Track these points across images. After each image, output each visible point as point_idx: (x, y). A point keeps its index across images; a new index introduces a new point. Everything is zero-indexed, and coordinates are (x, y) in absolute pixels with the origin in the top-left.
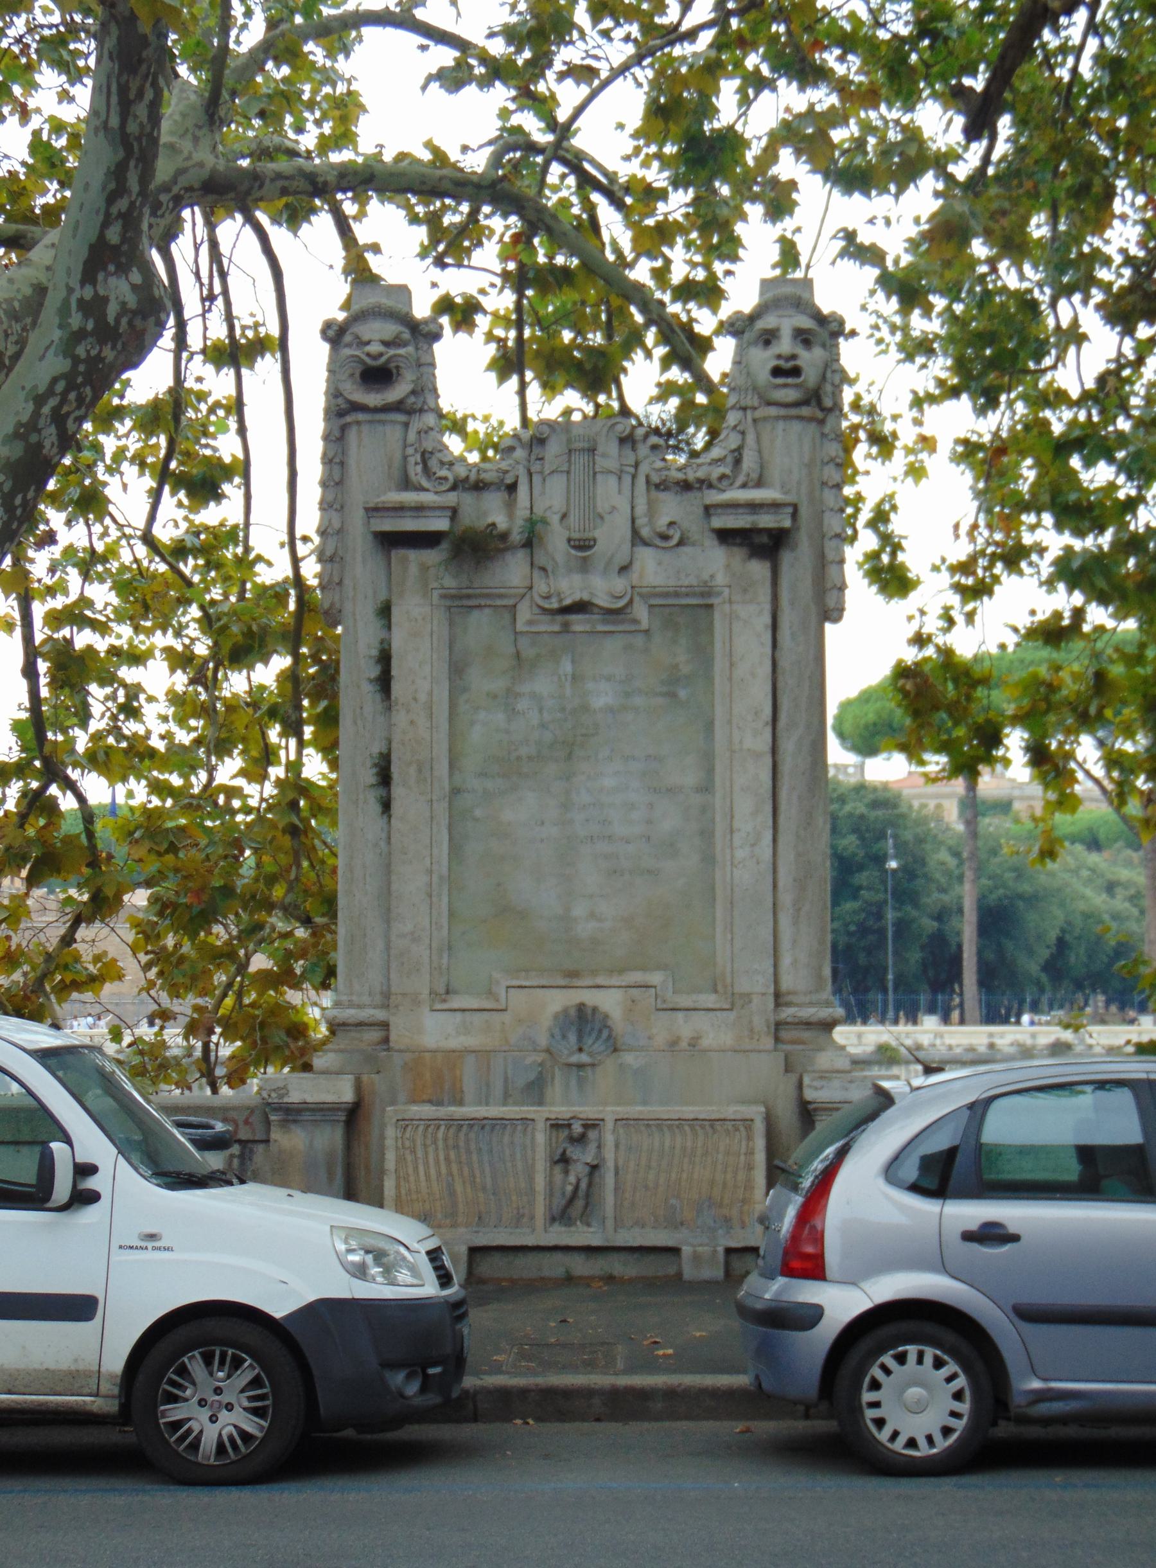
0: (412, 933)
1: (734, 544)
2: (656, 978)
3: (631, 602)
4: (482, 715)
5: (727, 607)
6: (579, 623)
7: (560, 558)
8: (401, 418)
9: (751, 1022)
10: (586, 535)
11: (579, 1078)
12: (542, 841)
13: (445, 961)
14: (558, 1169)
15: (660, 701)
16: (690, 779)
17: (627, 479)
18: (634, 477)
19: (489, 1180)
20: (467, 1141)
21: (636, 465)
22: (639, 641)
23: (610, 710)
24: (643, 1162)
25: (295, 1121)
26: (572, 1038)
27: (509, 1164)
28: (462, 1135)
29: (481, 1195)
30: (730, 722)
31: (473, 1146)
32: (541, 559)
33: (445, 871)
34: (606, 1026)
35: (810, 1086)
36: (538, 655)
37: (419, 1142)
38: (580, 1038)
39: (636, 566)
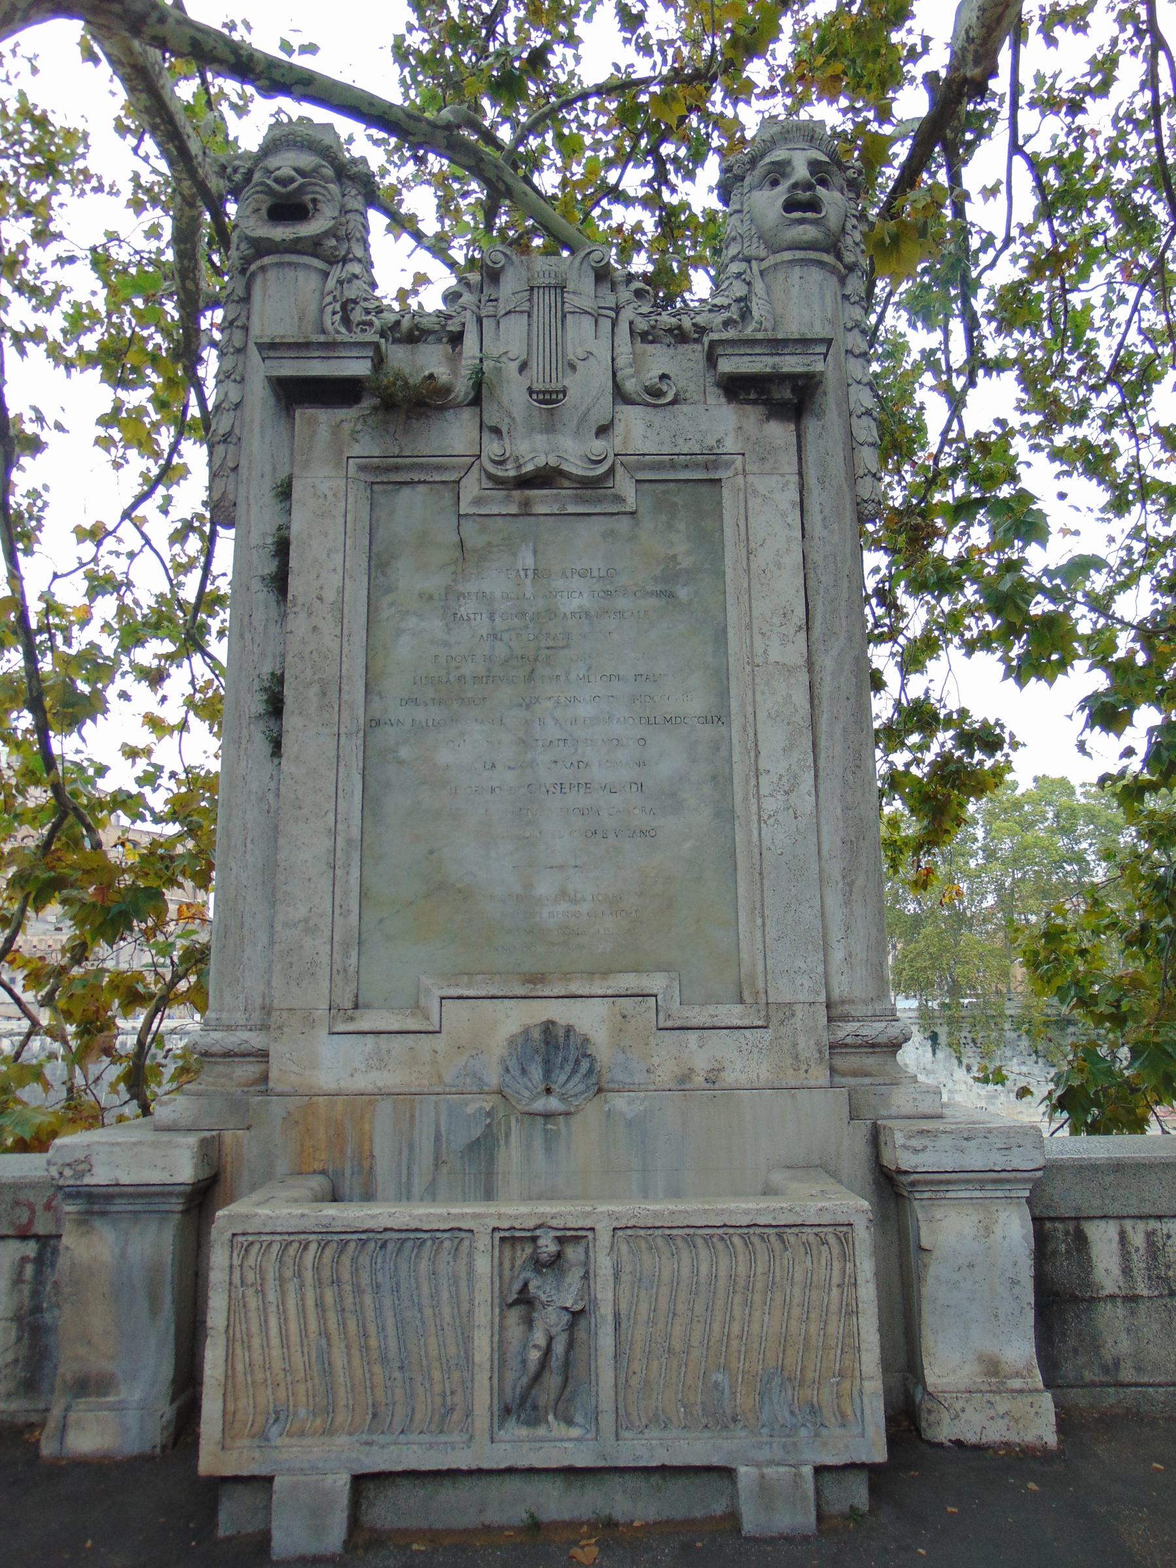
0: (306, 921)
1: (748, 402)
2: (656, 983)
3: (611, 471)
4: (412, 622)
5: (740, 480)
6: (543, 500)
7: (518, 413)
9: (795, 1045)
10: (554, 386)
11: (546, 1131)
12: (493, 790)
13: (353, 960)
14: (514, 1316)
15: (654, 602)
16: (696, 705)
17: (606, 324)
18: (614, 324)
19: (392, 1343)
20: (355, 1272)
21: (617, 310)
22: (623, 525)
24: (663, 1303)
25: (103, 1214)
26: (536, 1072)
27: (428, 1312)
28: (346, 1260)
29: (377, 1369)
30: (749, 627)
31: (365, 1280)
32: (492, 416)
33: (355, 833)
34: (585, 1055)
35: (904, 1147)
36: (489, 544)
37: (271, 1275)
38: (547, 1072)
39: (619, 428)
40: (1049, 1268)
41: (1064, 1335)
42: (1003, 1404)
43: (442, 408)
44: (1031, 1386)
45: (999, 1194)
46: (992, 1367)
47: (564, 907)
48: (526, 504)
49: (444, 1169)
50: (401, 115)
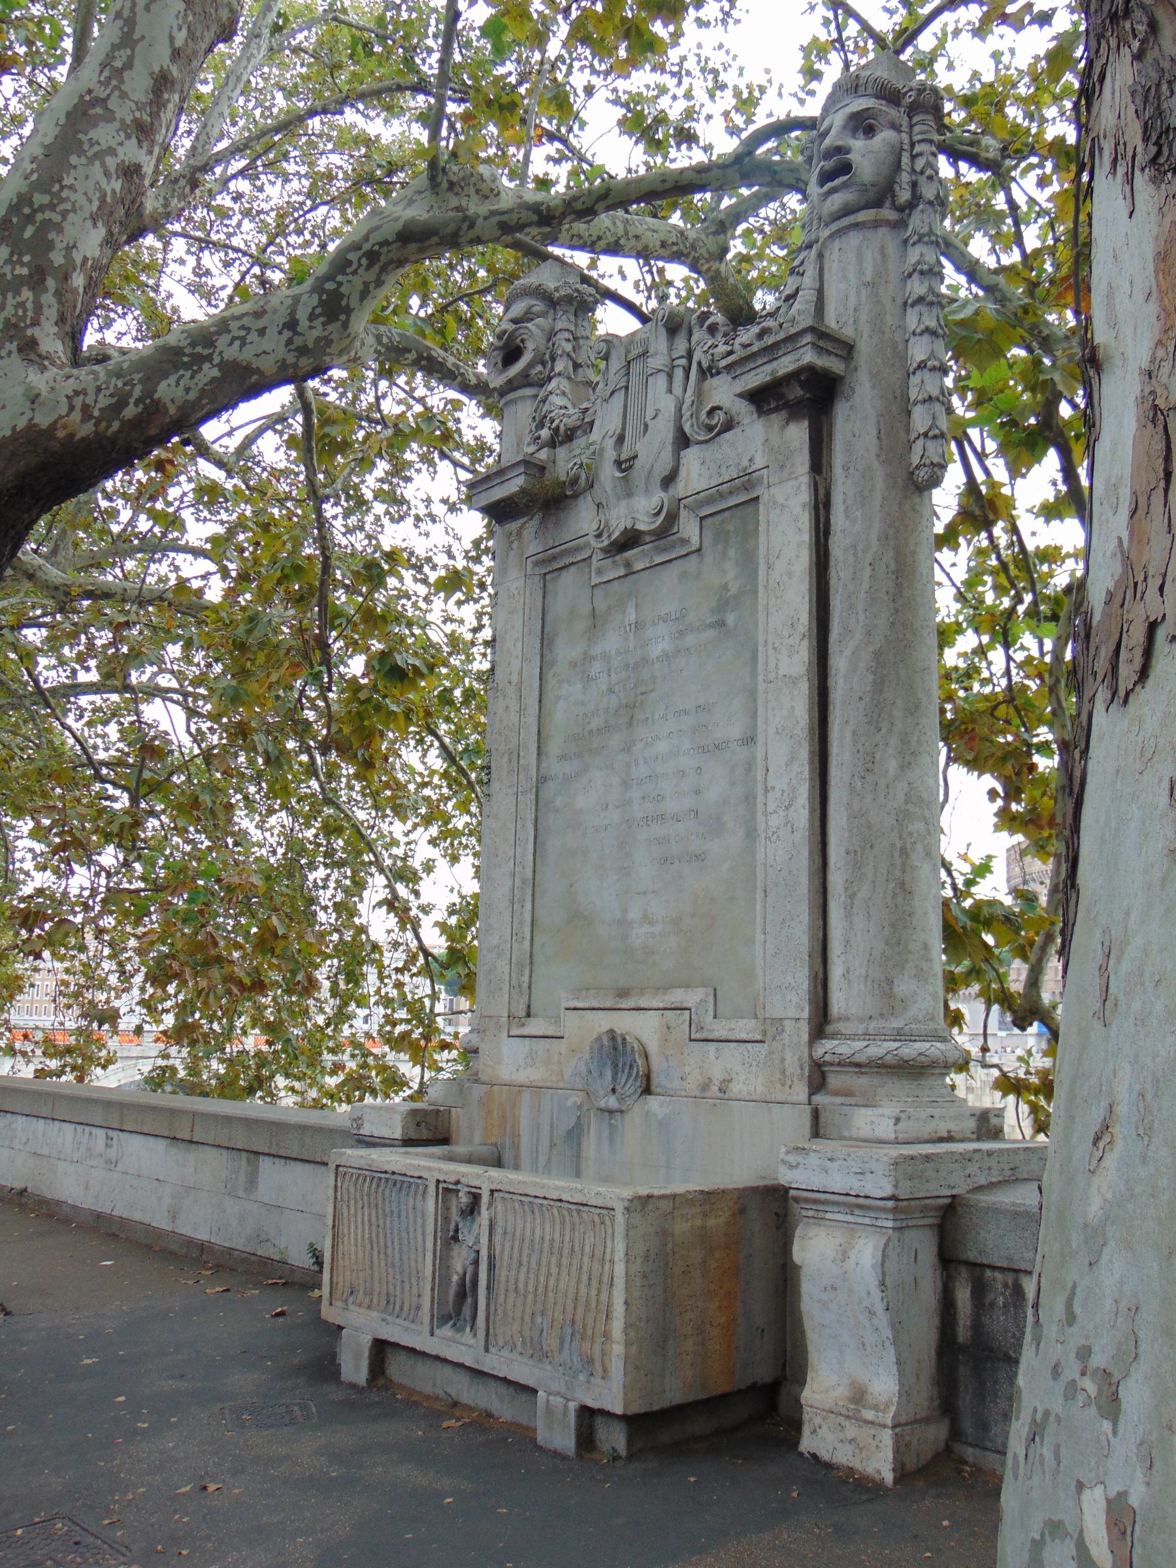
2: (692, 998)
6: (638, 557)
8: (529, 391)
9: (783, 1060)
13: (526, 978)
15: (710, 633)
16: (736, 730)
17: (679, 374)
22: (692, 563)
23: (667, 657)
40: (985, 1320)
41: (996, 1396)
42: (851, 1431)
43: (575, 496)
44: (880, 1420)
45: (867, 1221)
46: (859, 1396)
47: (646, 929)
48: (628, 564)
49: (555, 1152)
50: (692, 175)
